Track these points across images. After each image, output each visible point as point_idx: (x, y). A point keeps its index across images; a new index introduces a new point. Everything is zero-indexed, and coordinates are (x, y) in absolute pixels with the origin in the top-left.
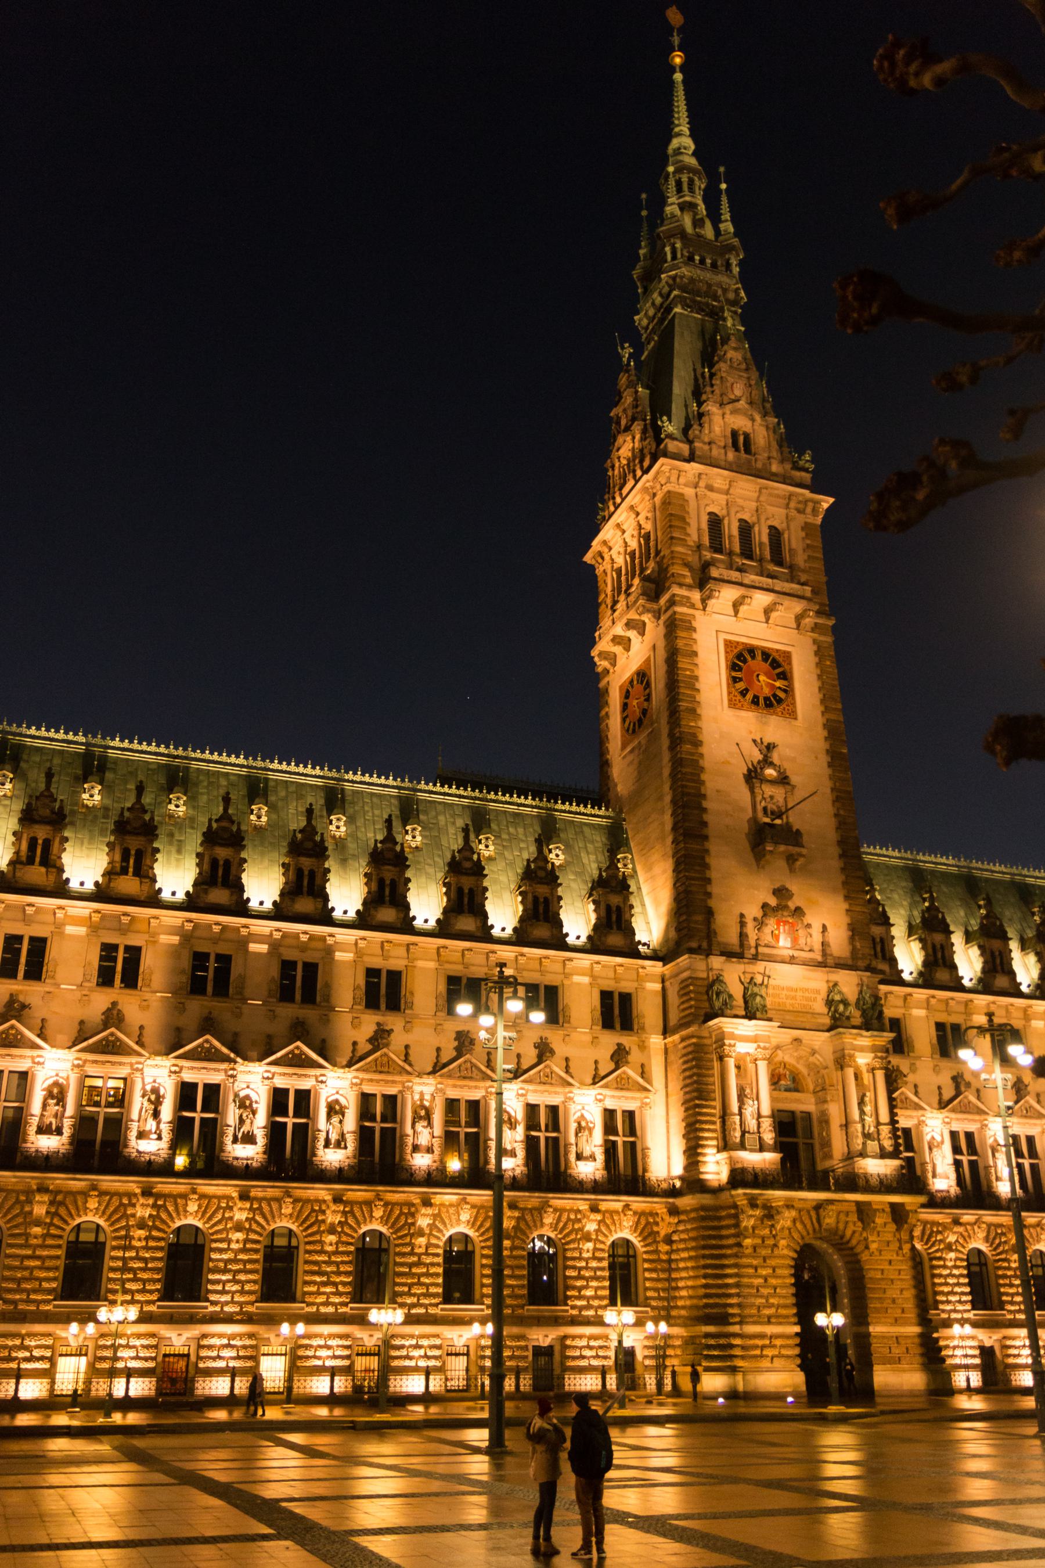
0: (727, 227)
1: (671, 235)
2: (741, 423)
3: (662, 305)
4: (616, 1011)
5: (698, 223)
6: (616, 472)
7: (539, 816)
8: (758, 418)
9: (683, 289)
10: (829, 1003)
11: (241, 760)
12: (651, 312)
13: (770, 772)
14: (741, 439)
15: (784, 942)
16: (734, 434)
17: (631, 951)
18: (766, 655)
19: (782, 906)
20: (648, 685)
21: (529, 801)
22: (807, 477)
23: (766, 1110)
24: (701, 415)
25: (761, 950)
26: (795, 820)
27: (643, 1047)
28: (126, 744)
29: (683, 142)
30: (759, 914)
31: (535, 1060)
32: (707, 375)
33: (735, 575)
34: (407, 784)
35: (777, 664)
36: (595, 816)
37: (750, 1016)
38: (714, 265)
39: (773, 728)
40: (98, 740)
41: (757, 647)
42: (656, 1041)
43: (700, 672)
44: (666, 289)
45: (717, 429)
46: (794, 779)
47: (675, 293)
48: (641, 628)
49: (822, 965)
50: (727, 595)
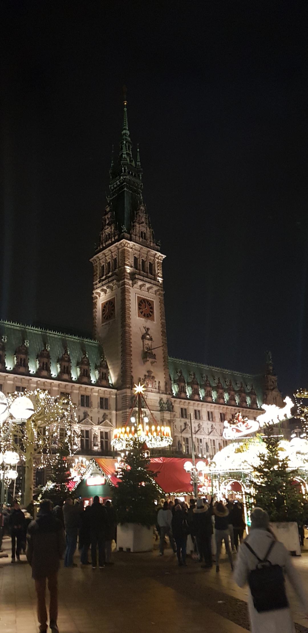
1: (124, 164)
2: (144, 229)
3: (119, 185)
4: (104, 403)
5: (131, 161)
6: (103, 236)
8: (148, 229)
10: (160, 403)
12: (115, 186)
13: (148, 336)
20: (114, 306)
21: (77, 338)
24: (133, 226)
27: (110, 414)
30: (144, 378)
31: (103, 419)
33: (142, 278)
34: (44, 331)
35: (150, 304)
38: (135, 176)
39: (149, 324)
42: (114, 412)
44: (122, 181)
46: (153, 339)
47: (125, 183)
49: (159, 393)
50: (140, 283)
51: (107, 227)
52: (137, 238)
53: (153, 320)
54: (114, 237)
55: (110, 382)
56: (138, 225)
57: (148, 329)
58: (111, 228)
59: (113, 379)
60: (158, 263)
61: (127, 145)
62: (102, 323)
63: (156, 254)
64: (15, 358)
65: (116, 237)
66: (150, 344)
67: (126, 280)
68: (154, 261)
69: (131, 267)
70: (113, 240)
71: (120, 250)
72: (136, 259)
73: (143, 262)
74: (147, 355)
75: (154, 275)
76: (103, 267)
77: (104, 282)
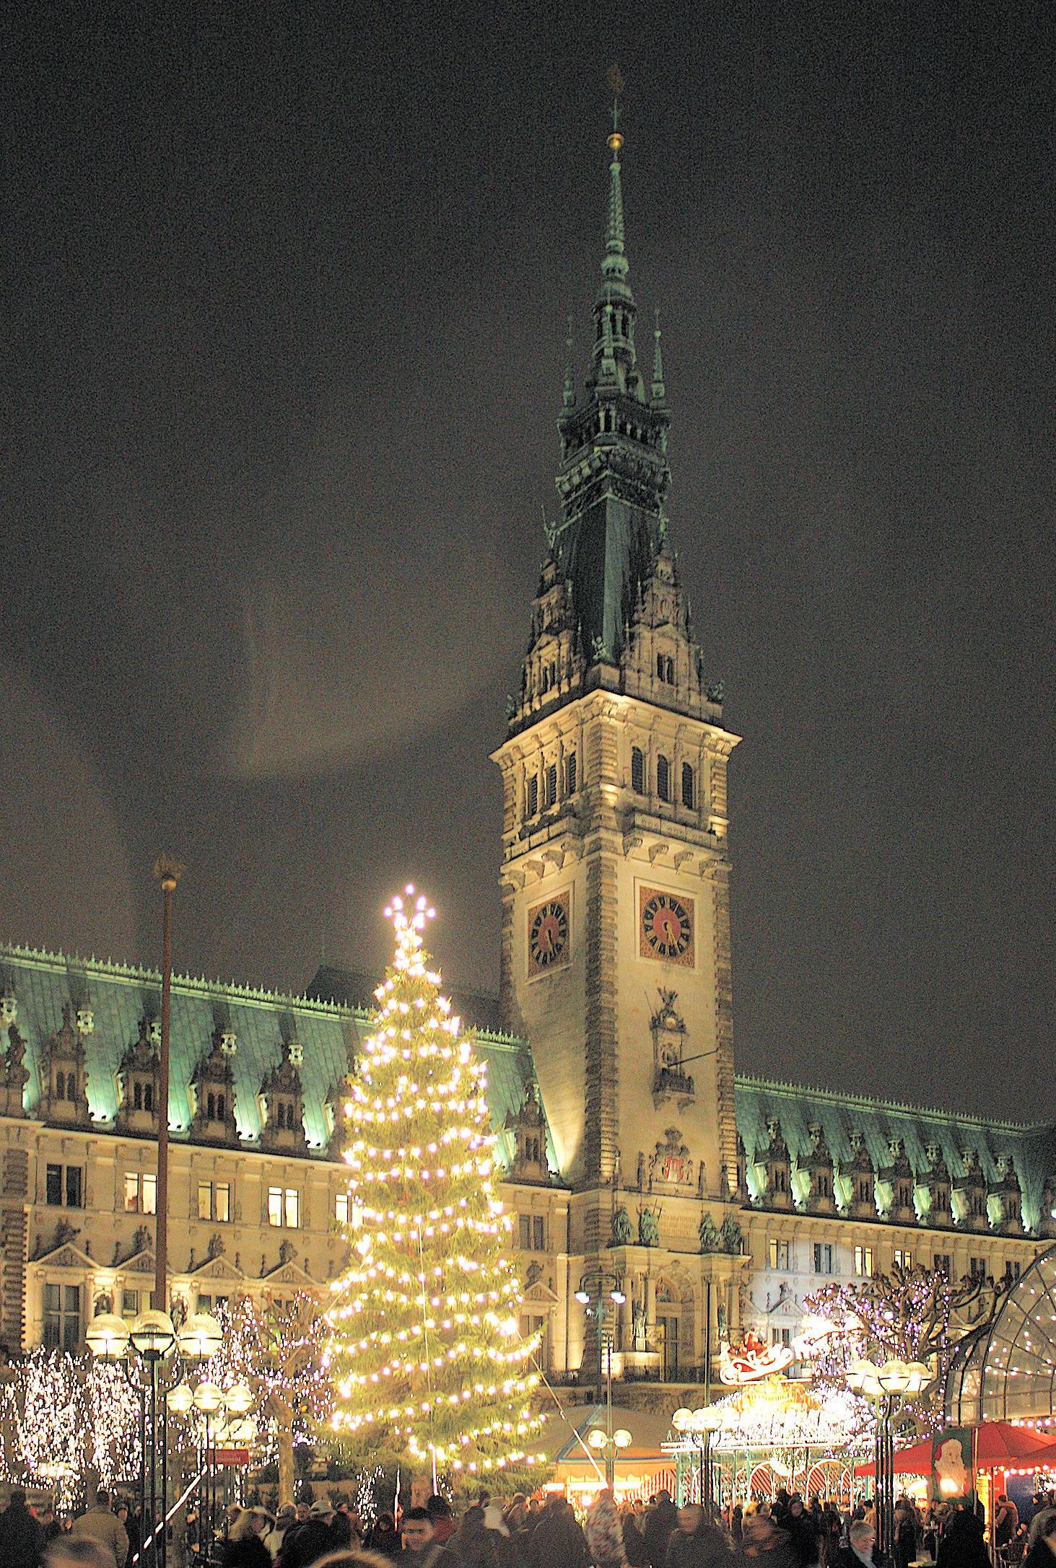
2: (667, 647)
3: (589, 477)
5: (631, 382)
6: (535, 670)
8: (682, 643)
10: (702, 1229)
11: (202, 984)
12: (576, 480)
13: (671, 1020)
15: (672, 1177)
18: (673, 903)
20: (564, 921)
26: (688, 1069)
27: (552, 1263)
28: (101, 966)
32: (640, 589)
33: (654, 822)
38: (644, 439)
40: (76, 961)
41: (667, 895)
44: (597, 464)
45: (645, 654)
46: (688, 1026)
47: (607, 472)
51: (545, 638)
52: (645, 681)
54: (569, 677)
55: (552, 1167)
56: (646, 633)
57: (672, 996)
58: (560, 645)
59: (561, 1153)
60: (714, 763)
61: (619, 318)
62: (531, 974)
64: (264, 1105)
66: (676, 1045)
67: (603, 834)
68: (700, 759)
70: (565, 689)
71: (587, 727)
72: (638, 758)
74: (669, 1079)
77: (535, 839)
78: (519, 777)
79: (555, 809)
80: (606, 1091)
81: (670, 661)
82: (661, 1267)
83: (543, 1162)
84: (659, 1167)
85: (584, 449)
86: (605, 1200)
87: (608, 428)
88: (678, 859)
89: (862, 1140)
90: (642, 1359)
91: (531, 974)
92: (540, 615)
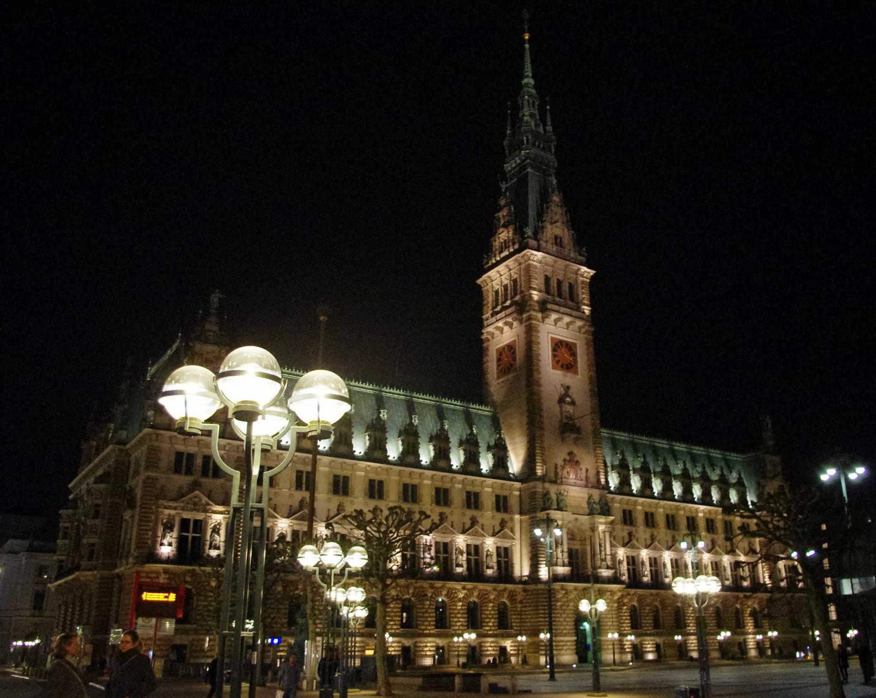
0: (549, 128)
3: (519, 164)
4: (501, 504)
5: (537, 126)
7: (463, 411)
8: (566, 230)
9: (530, 159)
10: (589, 503)
12: (514, 165)
13: (568, 399)
14: (558, 241)
15: (572, 476)
16: (556, 238)
17: (507, 477)
19: (572, 461)
20: (514, 353)
22: (584, 259)
23: (566, 549)
24: (543, 227)
25: (564, 480)
26: (578, 423)
27: (512, 519)
29: (529, 81)
30: (562, 463)
33: (556, 307)
34: (408, 394)
35: (570, 348)
36: (484, 411)
37: (560, 509)
38: (544, 148)
39: (569, 379)
43: (541, 352)
44: (523, 158)
46: (577, 403)
48: (510, 325)
49: (586, 486)
50: (554, 316)
51: (501, 230)
52: (549, 246)
53: (576, 372)
54: (514, 244)
55: (511, 471)
56: (549, 226)
57: (568, 388)
59: (515, 465)
60: (583, 282)
61: (531, 101)
62: (498, 378)
63: (579, 269)
65: (516, 246)
66: (571, 411)
67: (533, 313)
68: (576, 280)
69: (540, 291)
70: (512, 250)
72: (547, 280)
73: (559, 283)
74: (568, 428)
75: (578, 303)
76: (497, 292)
77: (499, 316)
78: (490, 291)
79: (508, 303)
80: (538, 433)
81: (561, 238)
82: (569, 522)
83: (506, 468)
84: (566, 471)
85: (517, 152)
86: (539, 487)
87: (528, 143)
88: (568, 324)
89: (665, 460)
90: (561, 570)
91: (498, 378)
92: (499, 220)
